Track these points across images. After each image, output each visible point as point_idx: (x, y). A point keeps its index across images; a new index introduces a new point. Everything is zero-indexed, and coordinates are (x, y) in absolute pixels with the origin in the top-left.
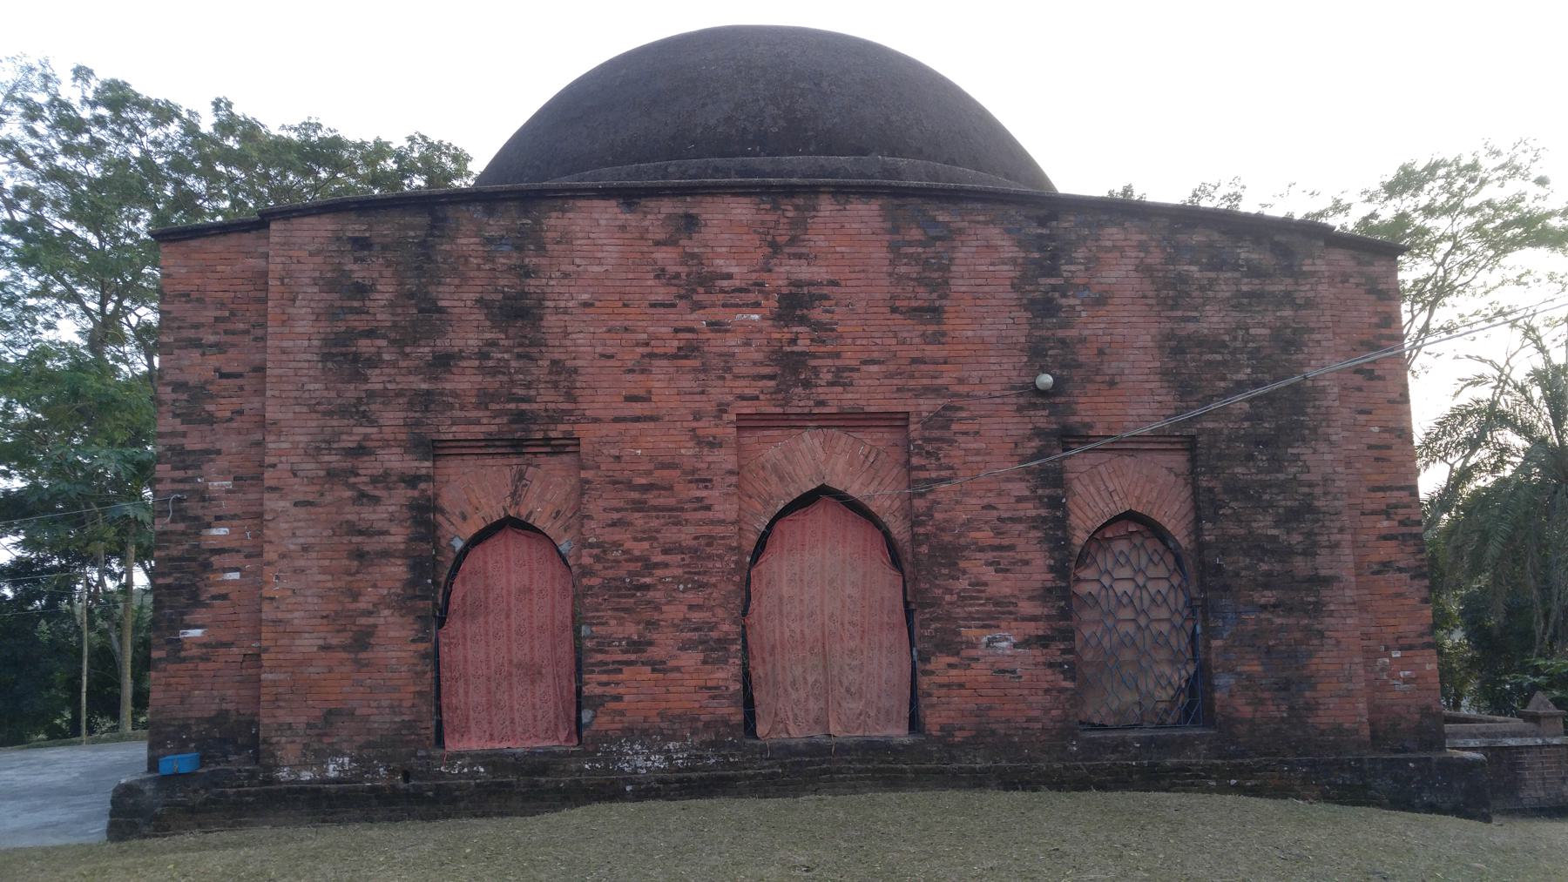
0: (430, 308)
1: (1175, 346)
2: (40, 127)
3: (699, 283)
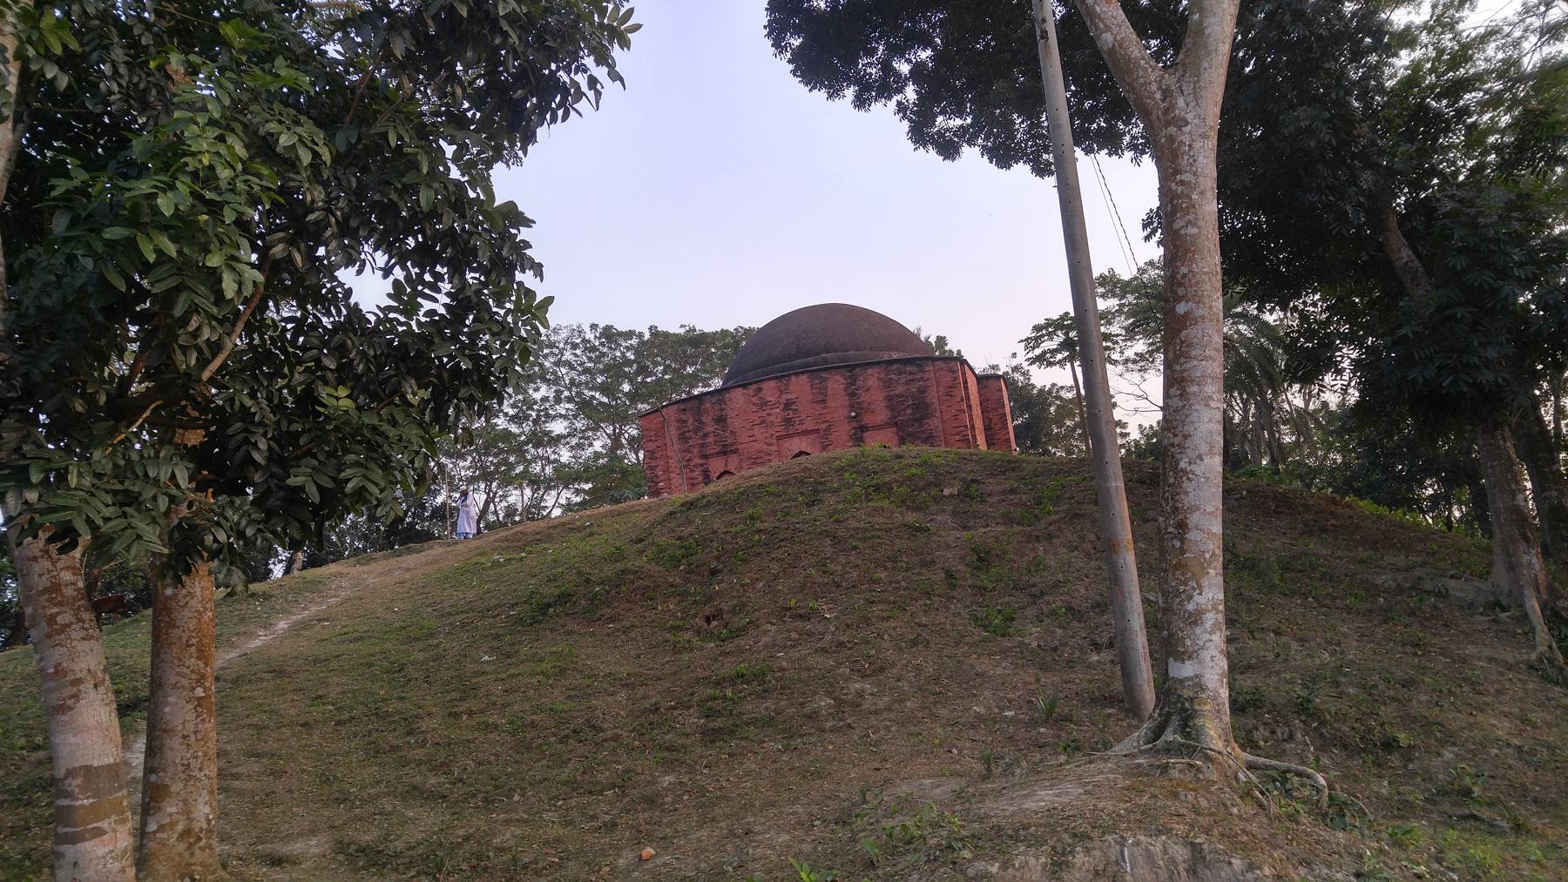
0: (701, 423)
1: (890, 398)
2: (578, 352)
3: (763, 404)
